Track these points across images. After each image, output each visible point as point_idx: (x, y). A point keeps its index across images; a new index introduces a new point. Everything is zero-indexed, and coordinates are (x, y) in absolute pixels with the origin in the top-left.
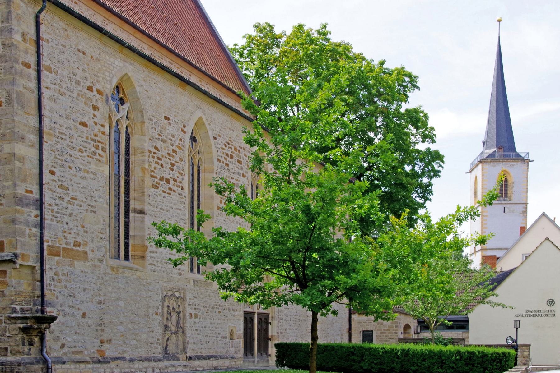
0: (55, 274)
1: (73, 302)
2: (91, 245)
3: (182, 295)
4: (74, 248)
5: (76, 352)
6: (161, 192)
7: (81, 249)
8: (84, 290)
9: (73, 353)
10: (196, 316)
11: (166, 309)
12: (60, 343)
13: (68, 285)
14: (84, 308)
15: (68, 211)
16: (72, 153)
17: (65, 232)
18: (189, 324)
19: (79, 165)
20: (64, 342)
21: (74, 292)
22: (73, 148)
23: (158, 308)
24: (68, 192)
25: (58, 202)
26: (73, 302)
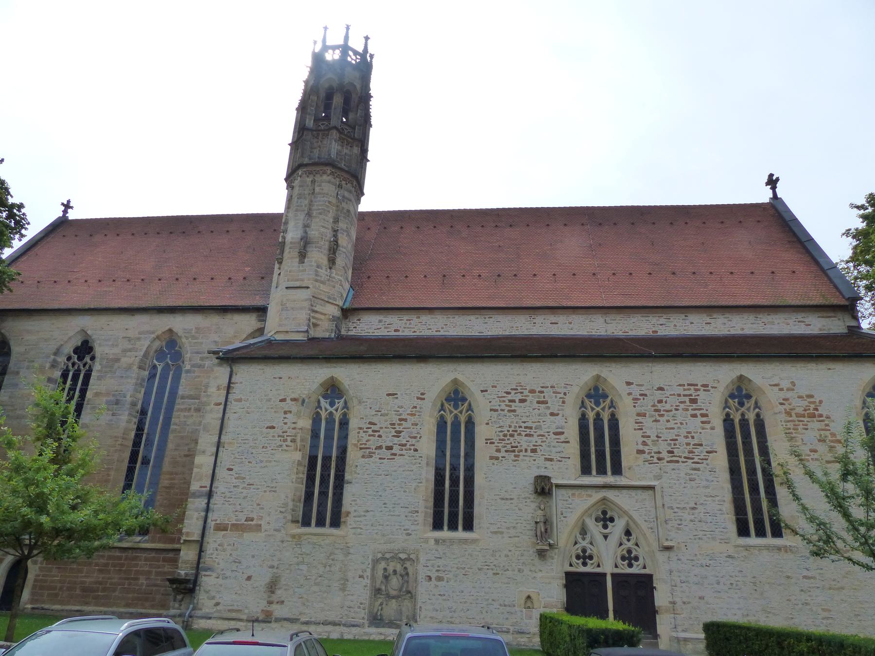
3: (413, 556)
5: (233, 610)
6: (378, 460)
8: (253, 556)
9: (229, 611)
10: (439, 579)
11: (380, 573)
12: (214, 602)
14: (249, 573)
18: (423, 590)
20: (220, 601)
21: (239, 559)
23: (364, 571)
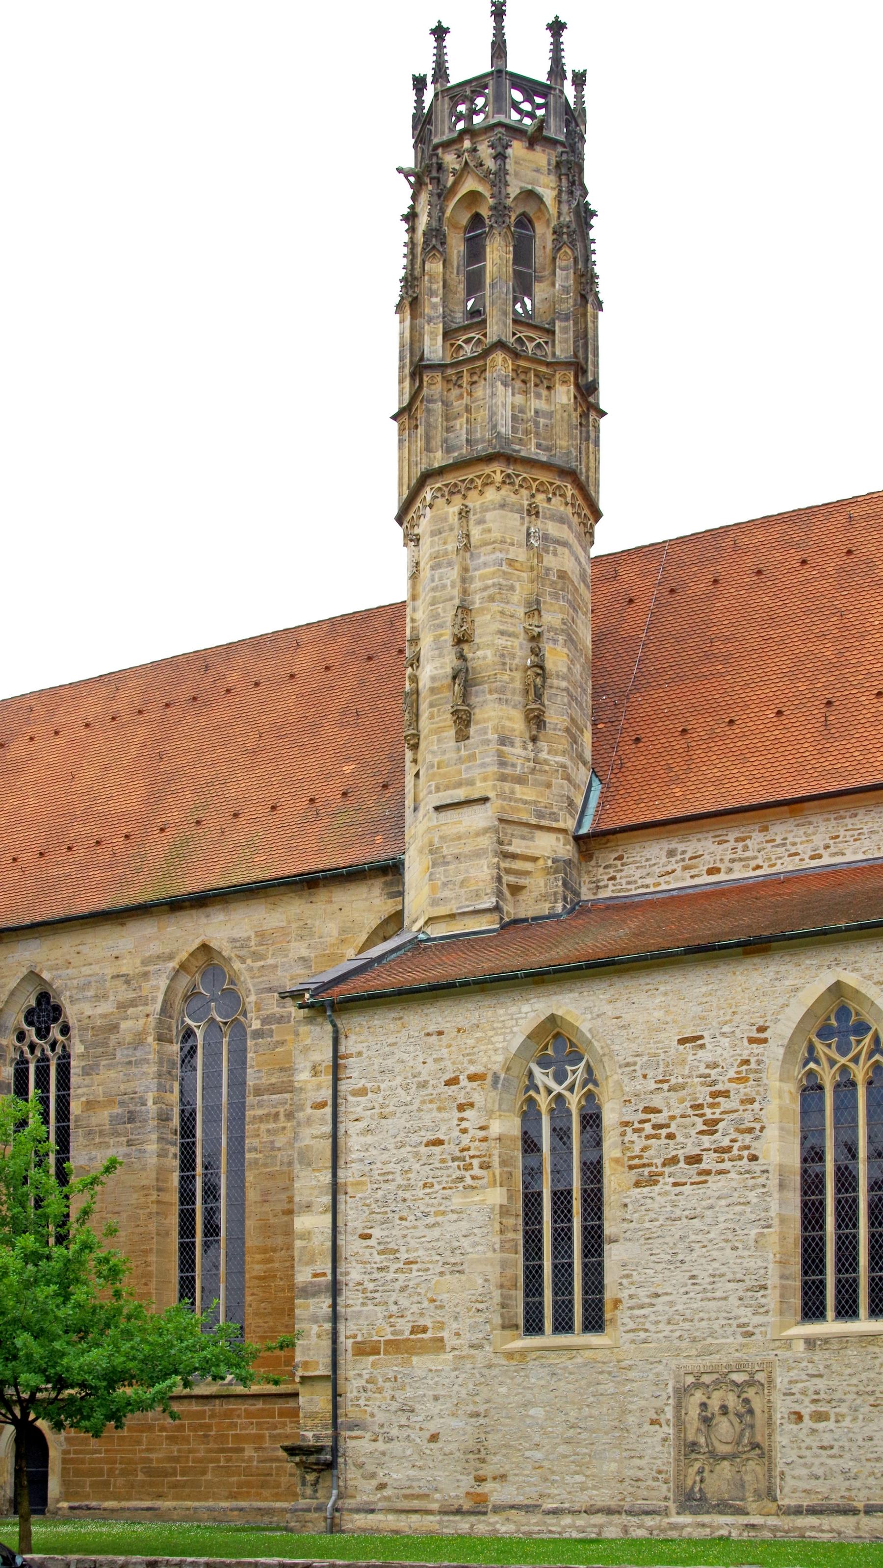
0: (367, 1382)
1: (408, 1419)
2: (455, 1326)
4: (413, 1337)
7: (428, 1335)
13: (399, 1395)
15: (397, 1286)
16: (407, 1195)
17: (391, 1316)
19: (422, 1208)
22: (407, 1188)
24: (397, 1255)
25: (376, 1275)
26: (408, 1419)
